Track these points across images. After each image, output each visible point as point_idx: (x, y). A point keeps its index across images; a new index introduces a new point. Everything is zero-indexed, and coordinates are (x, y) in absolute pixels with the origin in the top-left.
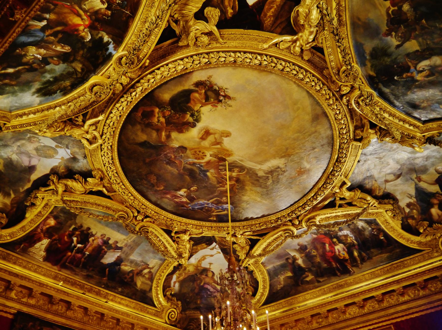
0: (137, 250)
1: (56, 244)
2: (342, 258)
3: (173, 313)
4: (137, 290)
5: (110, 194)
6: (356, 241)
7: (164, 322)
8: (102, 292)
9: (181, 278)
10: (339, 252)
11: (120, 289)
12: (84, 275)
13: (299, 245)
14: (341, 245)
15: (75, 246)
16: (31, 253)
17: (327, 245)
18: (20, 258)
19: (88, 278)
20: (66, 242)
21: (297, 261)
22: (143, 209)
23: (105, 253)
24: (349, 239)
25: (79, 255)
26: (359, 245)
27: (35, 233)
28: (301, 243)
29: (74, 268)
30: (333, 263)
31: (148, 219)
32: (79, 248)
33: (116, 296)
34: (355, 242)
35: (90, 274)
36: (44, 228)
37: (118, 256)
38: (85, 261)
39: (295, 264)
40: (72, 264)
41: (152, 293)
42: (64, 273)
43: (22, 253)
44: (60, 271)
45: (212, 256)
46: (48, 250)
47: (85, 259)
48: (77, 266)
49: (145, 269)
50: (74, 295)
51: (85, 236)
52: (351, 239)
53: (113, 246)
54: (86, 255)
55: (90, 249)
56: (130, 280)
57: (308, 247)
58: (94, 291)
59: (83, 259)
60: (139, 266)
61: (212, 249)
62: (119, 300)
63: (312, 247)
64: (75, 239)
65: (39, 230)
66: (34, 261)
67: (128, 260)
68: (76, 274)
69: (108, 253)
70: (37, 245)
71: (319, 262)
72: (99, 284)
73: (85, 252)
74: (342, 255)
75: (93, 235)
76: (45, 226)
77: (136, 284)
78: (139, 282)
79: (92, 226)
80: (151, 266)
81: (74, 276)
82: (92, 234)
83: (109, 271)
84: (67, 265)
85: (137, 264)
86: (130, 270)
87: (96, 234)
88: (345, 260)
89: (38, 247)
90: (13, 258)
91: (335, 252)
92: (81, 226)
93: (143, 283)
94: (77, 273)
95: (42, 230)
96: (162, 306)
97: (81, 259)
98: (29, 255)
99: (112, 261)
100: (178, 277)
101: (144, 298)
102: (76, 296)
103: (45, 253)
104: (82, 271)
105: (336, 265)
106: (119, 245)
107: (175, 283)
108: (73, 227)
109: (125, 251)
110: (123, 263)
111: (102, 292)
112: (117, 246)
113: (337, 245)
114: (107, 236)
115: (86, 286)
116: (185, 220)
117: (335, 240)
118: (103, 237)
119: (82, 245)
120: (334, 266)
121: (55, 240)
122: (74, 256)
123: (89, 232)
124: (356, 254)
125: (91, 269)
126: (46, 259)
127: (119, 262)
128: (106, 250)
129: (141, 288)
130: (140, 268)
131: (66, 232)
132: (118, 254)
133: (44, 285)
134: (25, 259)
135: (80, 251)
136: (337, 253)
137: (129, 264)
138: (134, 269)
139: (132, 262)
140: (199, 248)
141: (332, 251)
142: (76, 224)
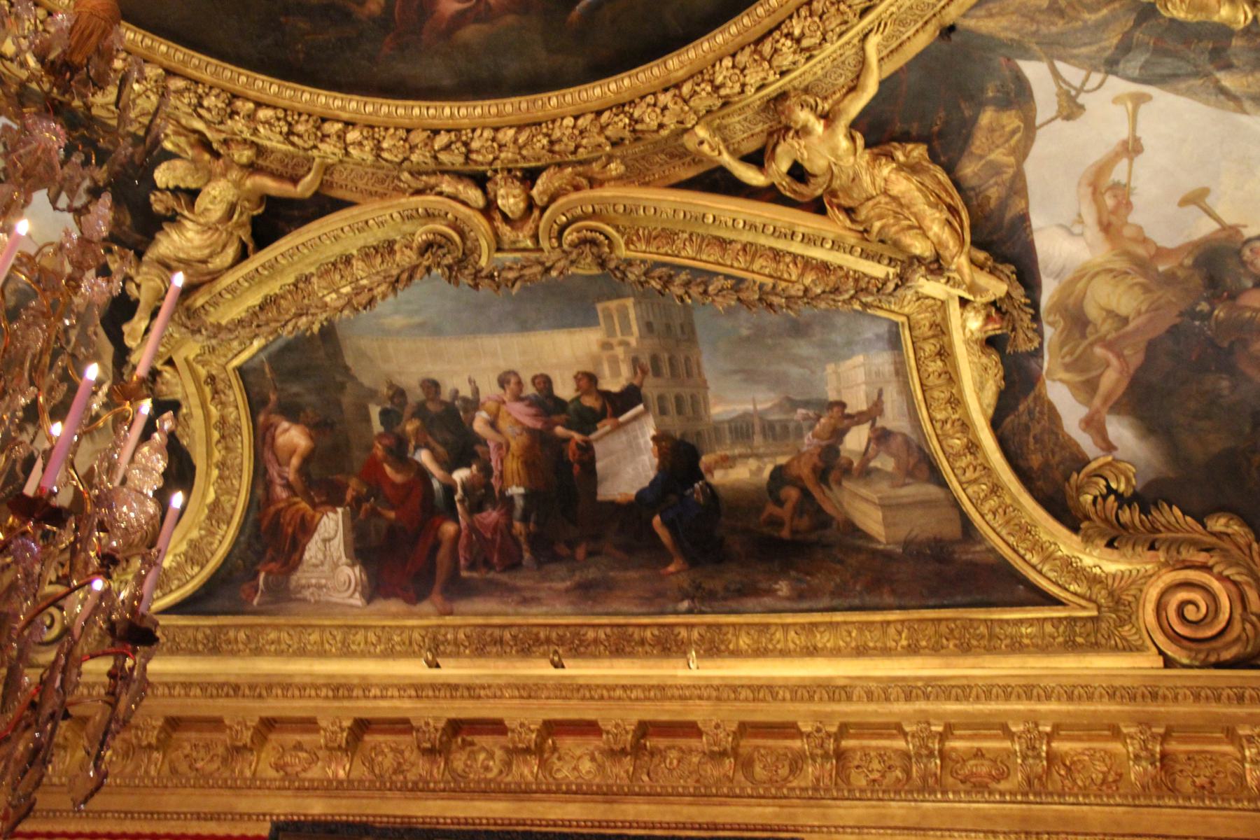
0: (711, 365)
1: (374, 513)
3: (1183, 595)
4: (888, 556)
5: (305, 188)
7: (1159, 662)
8: (684, 633)
9: (1111, 379)
11: (783, 588)
12: (567, 590)
15: (449, 489)
16: (307, 594)
18: (264, 626)
19: (587, 592)
20: (404, 485)
22: (447, 147)
23: (587, 450)
25: (491, 516)
27: (272, 509)
29: (504, 578)
31: (541, 183)
32: (468, 487)
33: (767, 626)
35: (592, 574)
36: (291, 473)
37: (654, 439)
38: (532, 526)
40: (488, 565)
41: (981, 539)
42: (474, 614)
43: (271, 607)
44: (451, 613)
45: (1132, 148)
46: (364, 549)
47: (525, 519)
48: (514, 565)
49: (838, 434)
50: (500, 687)
51: (451, 426)
53: (590, 401)
54: (519, 503)
55: (513, 465)
56: (804, 523)
58: (642, 642)
59: (518, 526)
60: (800, 435)
61: (1071, 108)
62: (802, 640)
64: (424, 457)
65: (281, 493)
66: (327, 616)
67: (717, 428)
68: (525, 601)
69: (598, 448)
70: (313, 551)
72: (657, 600)
73: (502, 492)
75: (473, 404)
76: (288, 464)
77: (853, 529)
78: (867, 511)
79: (433, 370)
80: (857, 402)
81: (523, 609)
82: (465, 400)
83: (666, 523)
84: (465, 580)
85: (775, 432)
86: (766, 474)
87: (476, 391)
89: (320, 556)
90: (242, 635)
92: (399, 394)
93: (886, 506)
94: (528, 594)
95: (288, 486)
96: (1094, 580)
97: (510, 526)
98: (304, 600)
99: (652, 474)
100: (1088, 388)
101: (955, 577)
102: (508, 686)
103: (357, 569)
104: (544, 578)
106: (613, 384)
107: (1093, 424)
108: (375, 411)
109: (661, 398)
110: (705, 460)
111: (684, 633)
112: (606, 395)
114: (526, 377)
115: (591, 634)
116: (676, 64)
118: (512, 385)
119: (469, 466)
121: (358, 500)
122: (472, 528)
123: (446, 395)
125: (581, 552)
126: (376, 589)
127: (680, 460)
128: (577, 437)
129: (902, 533)
130: (809, 442)
131: (370, 448)
132: (649, 429)
133: (350, 688)
134: (281, 620)
135: (481, 495)
137: (737, 451)
138: (782, 460)
139: (741, 429)
140: (998, 156)
142: (372, 394)
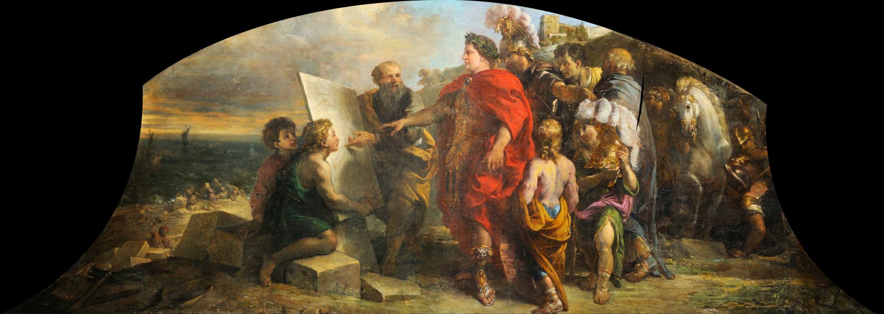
2: (537, 227)
6: (639, 175)
10: (539, 195)
13: (378, 74)
14: (566, 165)
17: (505, 137)
21: (317, 158)
24: (613, 154)
26: (641, 196)
28: (394, 70)
30: (485, 236)
34: (632, 177)
39: (299, 168)
52: (624, 157)
57: (417, 106)
63: (429, 117)
71: (420, 205)
74: (544, 215)
88: (545, 239)
91: (521, 187)
105: (495, 247)
113: (551, 156)
117: (553, 128)
120: (485, 249)
124: (608, 232)
136: (529, 196)
141: (512, 177)
